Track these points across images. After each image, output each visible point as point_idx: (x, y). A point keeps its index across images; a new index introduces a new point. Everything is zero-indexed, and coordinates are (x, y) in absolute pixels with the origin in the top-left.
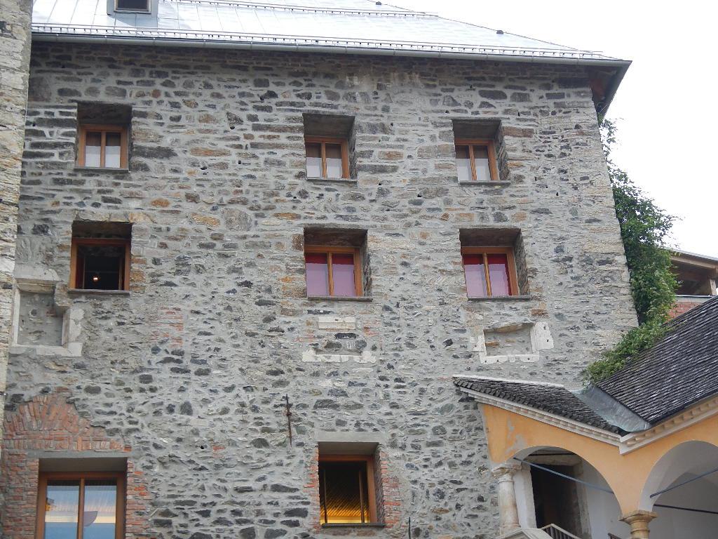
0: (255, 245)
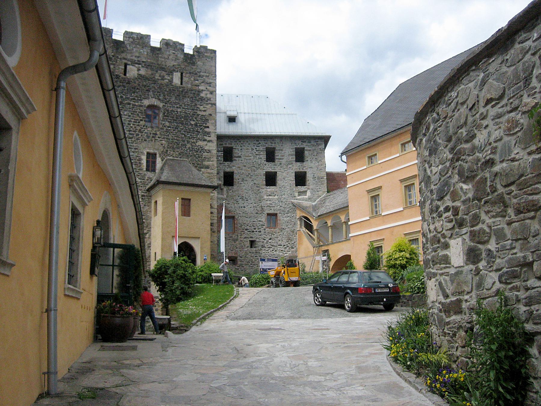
0: (256, 175)
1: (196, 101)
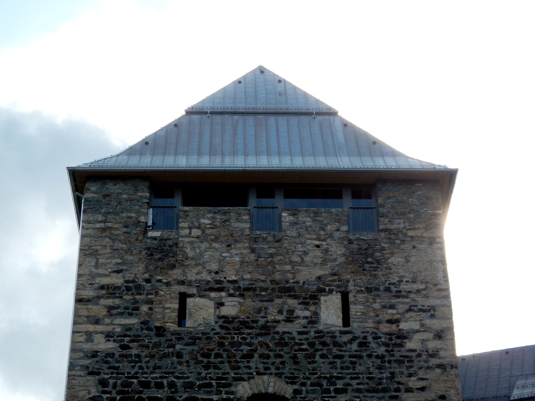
1: (394, 365)
